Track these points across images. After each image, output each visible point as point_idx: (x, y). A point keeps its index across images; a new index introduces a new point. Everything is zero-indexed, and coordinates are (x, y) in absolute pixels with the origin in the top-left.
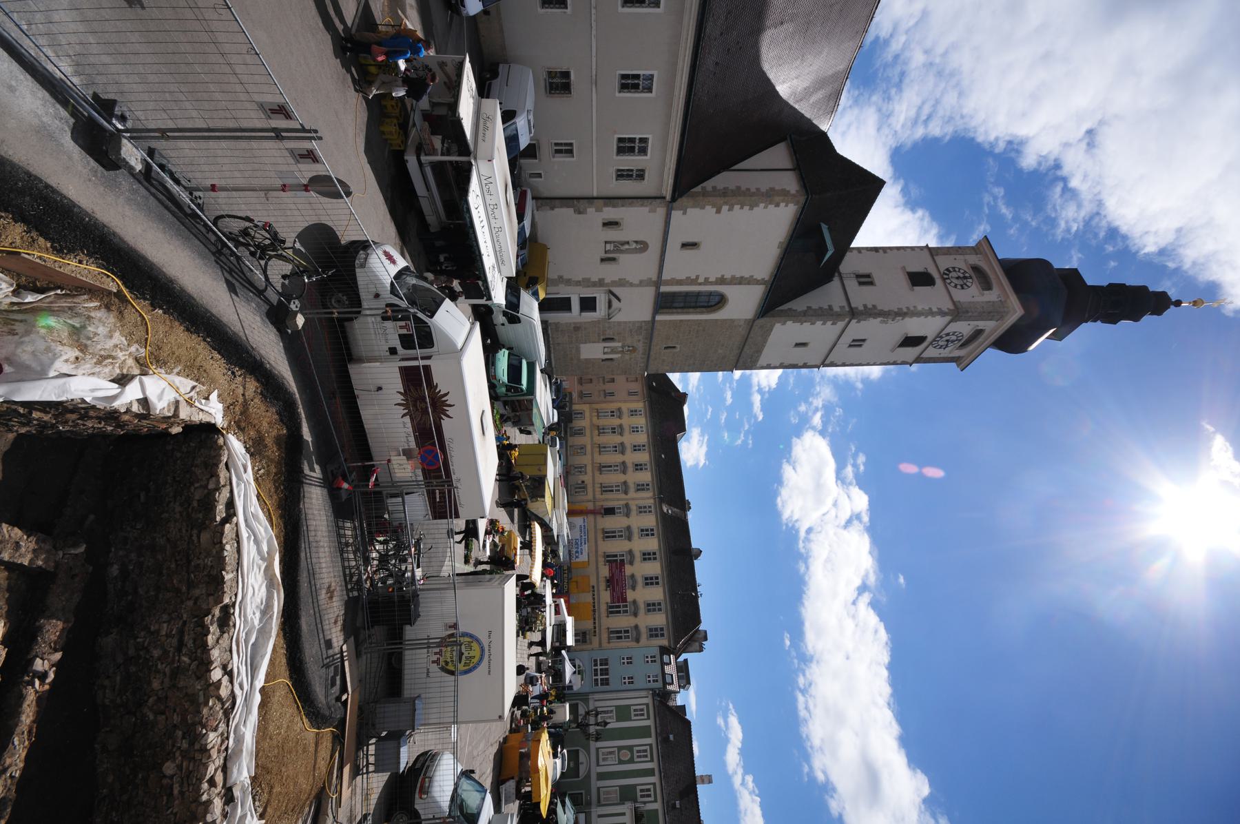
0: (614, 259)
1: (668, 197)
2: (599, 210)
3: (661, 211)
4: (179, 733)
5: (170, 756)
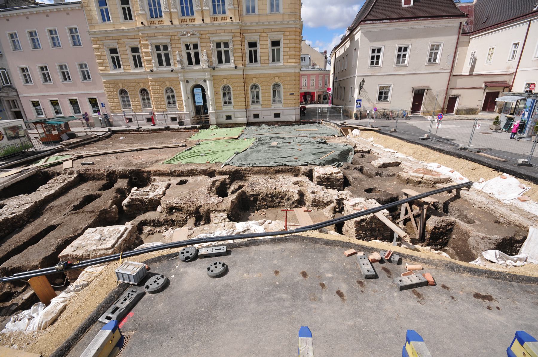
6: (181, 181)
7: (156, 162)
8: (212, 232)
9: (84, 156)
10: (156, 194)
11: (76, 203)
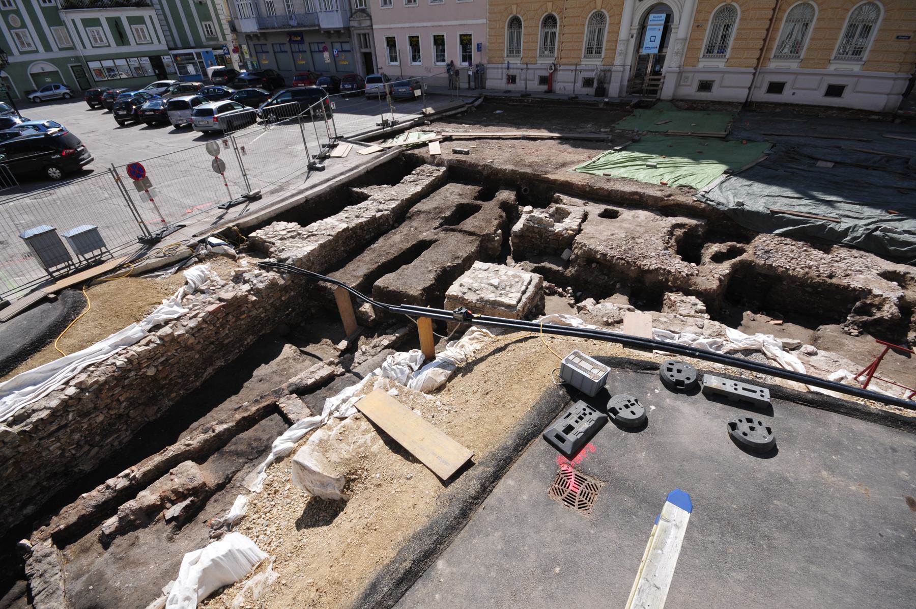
4: (126, 382)
5: (144, 377)
6: (606, 210)
7: (564, 165)
8: (677, 330)
9: (454, 137)
10: (567, 227)
11: (448, 213)
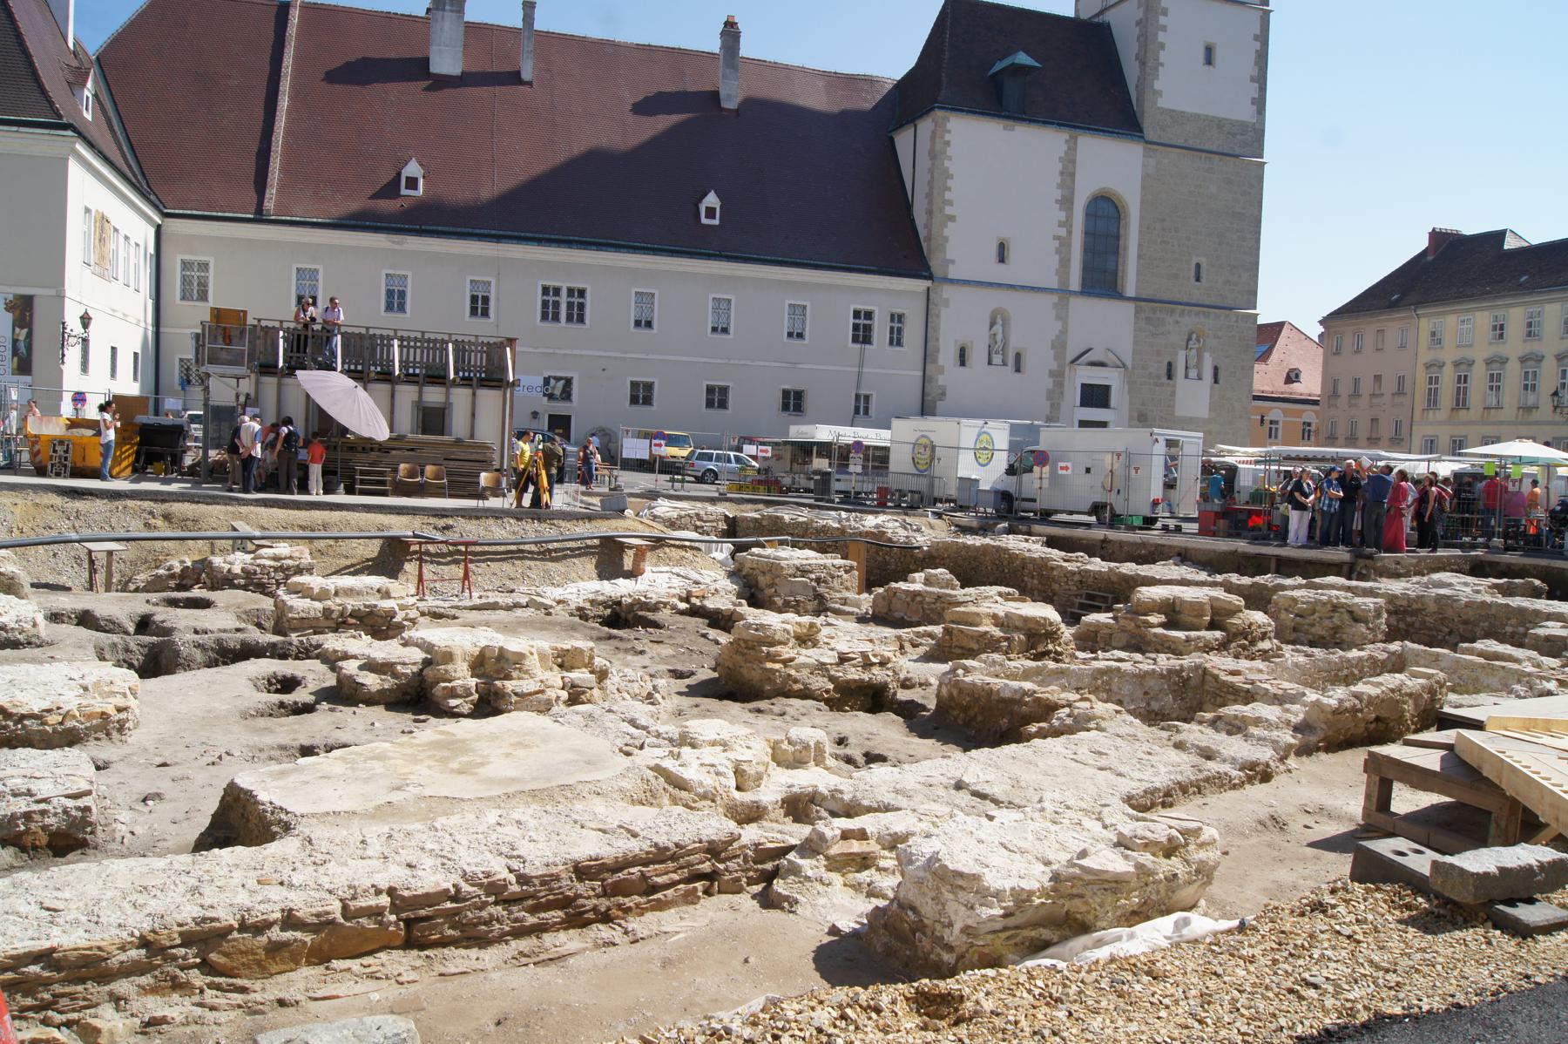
0: (1018, 357)
1: (928, 283)
2: (941, 371)
3: (947, 291)
